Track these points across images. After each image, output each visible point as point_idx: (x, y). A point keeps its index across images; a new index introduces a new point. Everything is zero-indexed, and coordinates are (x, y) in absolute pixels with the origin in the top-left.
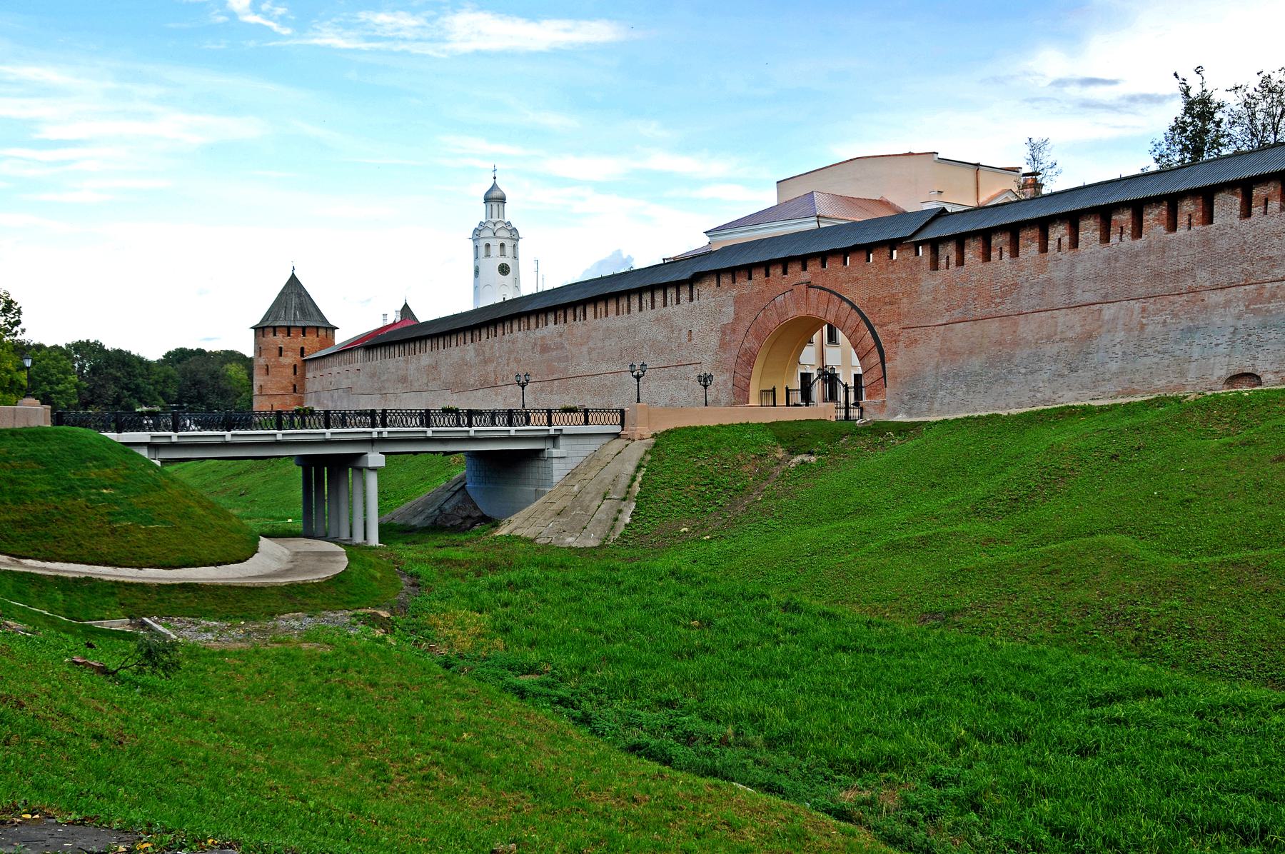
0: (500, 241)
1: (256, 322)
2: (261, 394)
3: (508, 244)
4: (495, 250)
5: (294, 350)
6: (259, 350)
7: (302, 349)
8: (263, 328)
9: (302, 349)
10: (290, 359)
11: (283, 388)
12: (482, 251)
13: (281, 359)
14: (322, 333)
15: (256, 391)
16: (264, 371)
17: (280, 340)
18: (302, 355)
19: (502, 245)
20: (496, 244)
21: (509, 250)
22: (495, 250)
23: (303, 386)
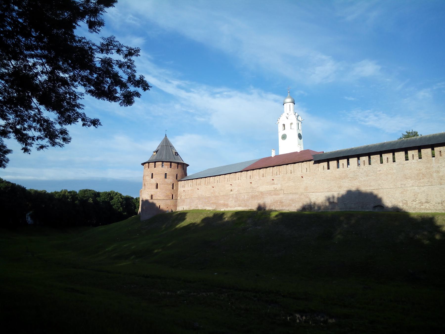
9: (177, 175)
10: (170, 180)
11: (166, 196)
16: (155, 186)
18: (177, 179)
23: (177, 196)
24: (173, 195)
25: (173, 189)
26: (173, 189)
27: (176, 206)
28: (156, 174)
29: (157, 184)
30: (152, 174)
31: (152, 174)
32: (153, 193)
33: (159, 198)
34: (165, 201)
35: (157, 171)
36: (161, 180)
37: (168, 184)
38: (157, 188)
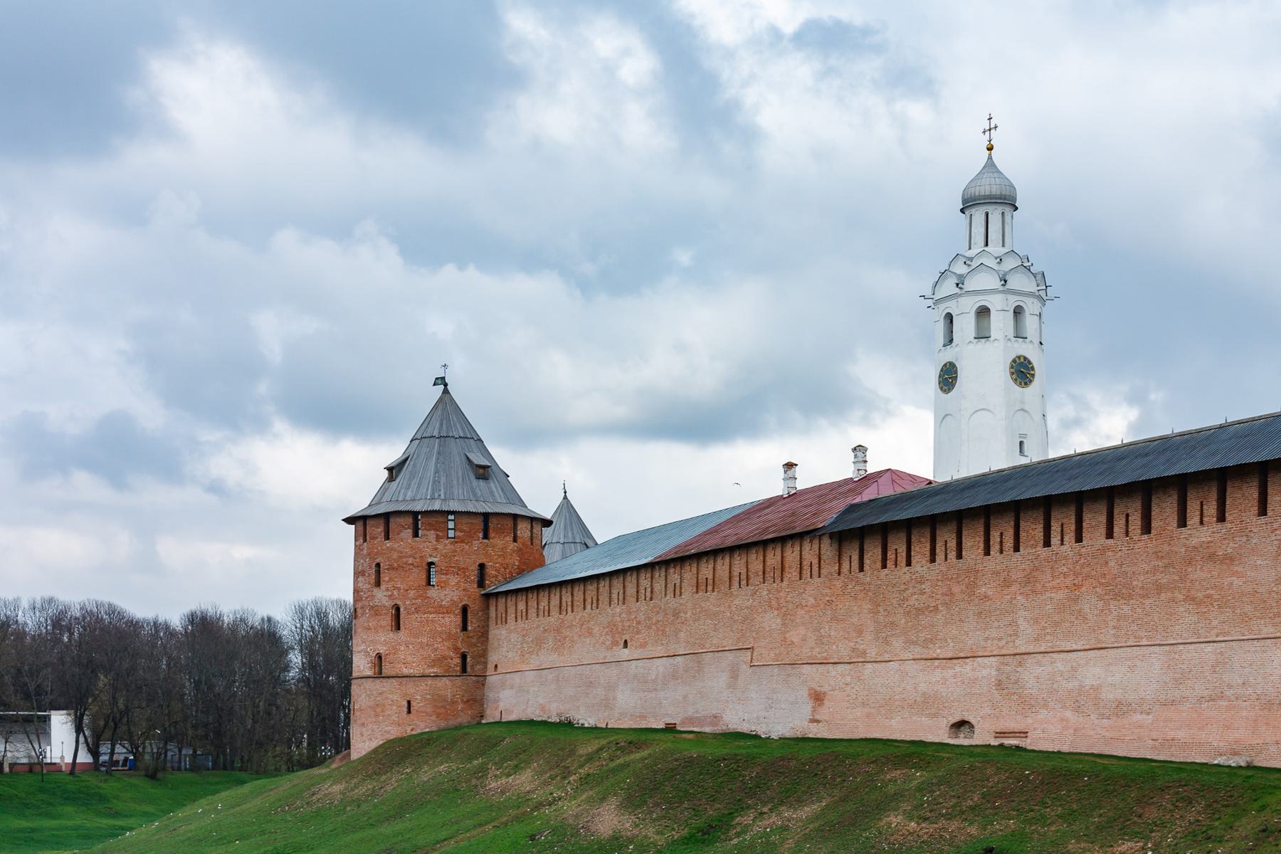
0: (1013, 301)
1: (359, 504)
2: (379, 675)
3: (1031, 306)
4: (1000, 323)
5: (462, 571)
6: (371, 572)
7: (482, 567)
8: (386, 516)
9: (482, 566)
10: (451, 591)
12: (965, 326)
13: (432, 593)
14: (523, 530)
15: (361, 664)
16: (387, 620)
17: (429, 545)
18: (481, 584)
19: (1018, 312)
20: (1000, 306)
21: (1030, 323)
22: (1000, 323)
23: (483, 656)
24: (464, 657)
25: (464, 628)
26: (464, 628)
27: (476, 701)
28: (391, 568)
29: (398, 609)
30: (378, 565)
31: (378, 565)
32: (382, 650)
33: (406, 671)
34: (429, 681)
35: (395, 555)
36: (412, 594)
37: (441, 610)
38: (398, 628)
